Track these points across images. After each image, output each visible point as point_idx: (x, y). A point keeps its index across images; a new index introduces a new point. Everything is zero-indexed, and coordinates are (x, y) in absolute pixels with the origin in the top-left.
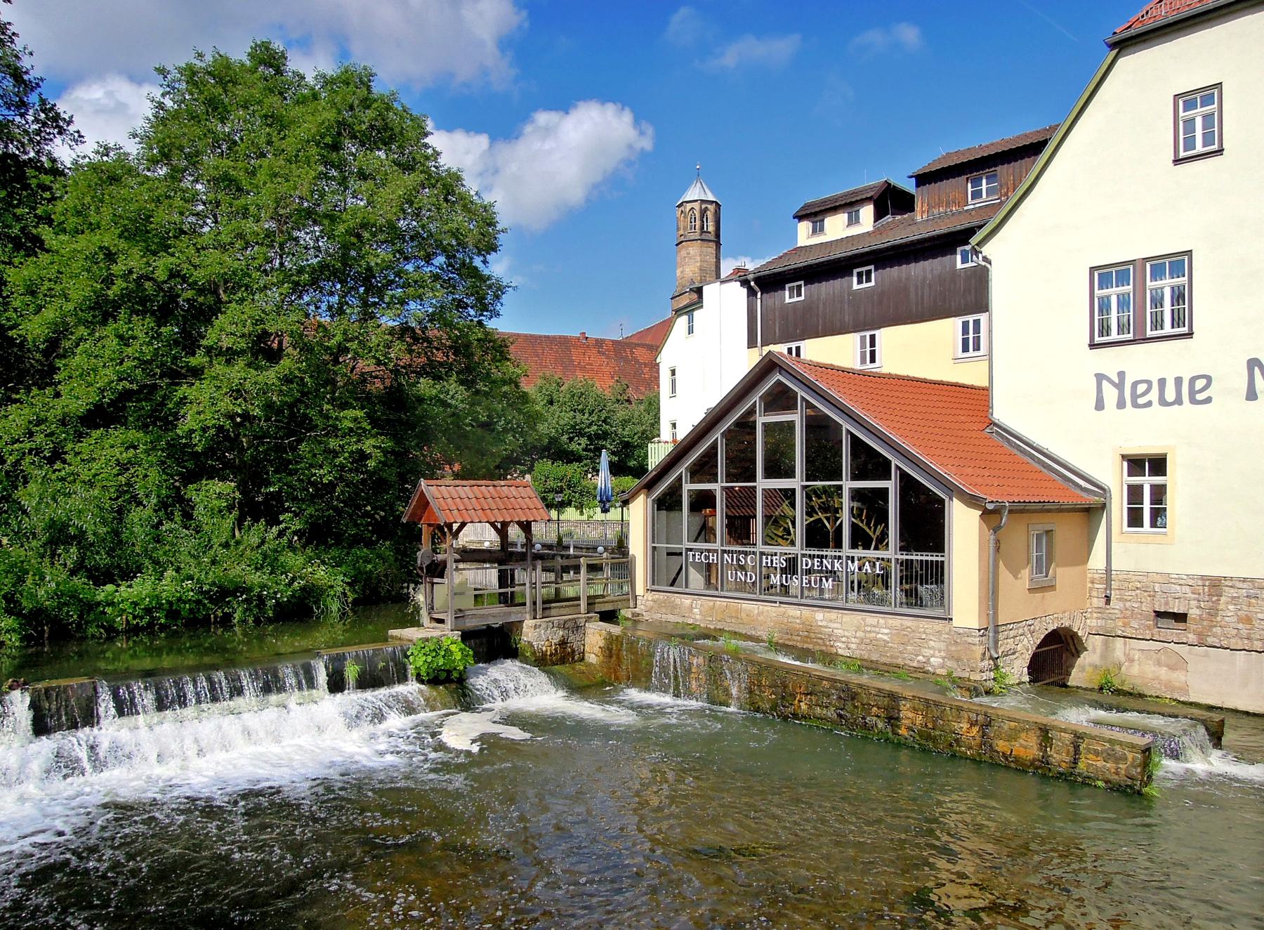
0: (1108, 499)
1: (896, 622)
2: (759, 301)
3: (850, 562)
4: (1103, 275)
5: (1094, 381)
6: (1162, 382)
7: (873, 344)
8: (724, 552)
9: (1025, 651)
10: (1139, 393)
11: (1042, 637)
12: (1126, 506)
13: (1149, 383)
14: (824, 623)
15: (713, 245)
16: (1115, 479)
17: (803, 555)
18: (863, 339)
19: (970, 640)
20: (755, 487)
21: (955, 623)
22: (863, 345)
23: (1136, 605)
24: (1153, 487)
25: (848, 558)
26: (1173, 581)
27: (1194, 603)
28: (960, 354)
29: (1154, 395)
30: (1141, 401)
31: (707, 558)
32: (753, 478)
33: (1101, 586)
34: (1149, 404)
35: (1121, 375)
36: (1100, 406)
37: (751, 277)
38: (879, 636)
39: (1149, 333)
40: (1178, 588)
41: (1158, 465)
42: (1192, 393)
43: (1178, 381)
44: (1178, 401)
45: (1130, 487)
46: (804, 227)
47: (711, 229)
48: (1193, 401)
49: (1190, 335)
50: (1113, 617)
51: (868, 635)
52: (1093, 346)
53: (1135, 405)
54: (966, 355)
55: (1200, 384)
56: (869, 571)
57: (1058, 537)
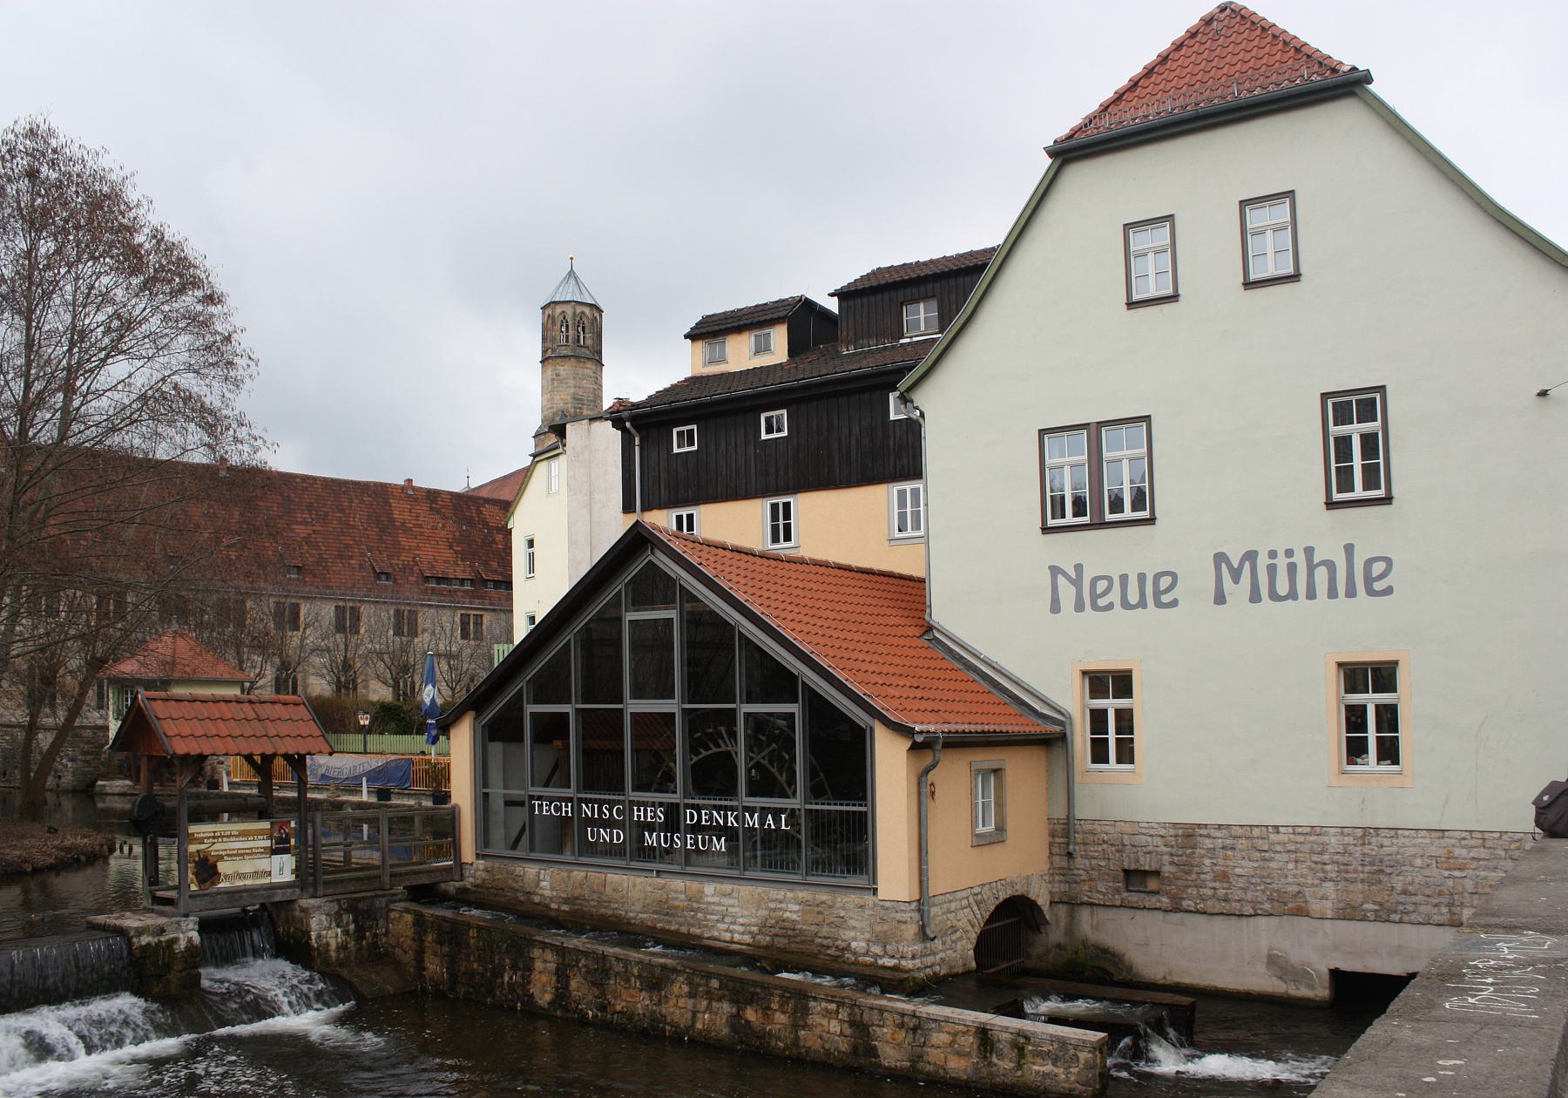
0: (1068, 727)
1: (803, 894)
3: (747, 814)
5: (1048, 574)
6: (1124, 579)
7: (787, 516)
8: (581, 800)
9: (970, 928)
10: (1099, 591)
11: (992, 908)
12: (1089, 736)
13: (1109, 579)
14: (715, 899)
16: (1072, 701)
17: (687, 806)
18: (774, 507)
19: (899, 916)
20: (622, 710)
21: (881, 894)
22: (775, 517)
23: (1103, 864)
24: (1118, 712)
25: (746, 809)
26: (1143, 831)
27: (1166, 858)
28: (897, 535)
29: (1116, 596)
31: (558, 809)
32: (619, 699)
33: (1062, 840)
34: (1110, 606)
35: (1079, 568)
36: (1055, 607)
38: (787, 915)
39: (1109, 517)
40: (1149, 839)
41: (1122, 683)
42: (1157, 594)
43: (1142, 578)
44: (1142, 603)
45: (1092, 711)
48: (1159, 604)
49: (1151, 520)
50: (1078, 879)
51: (772, 914)
52: (1046, 530)
53: (1095, 607)
55: (1165, 582)
56: (773, 827)
57: (1010, 776)
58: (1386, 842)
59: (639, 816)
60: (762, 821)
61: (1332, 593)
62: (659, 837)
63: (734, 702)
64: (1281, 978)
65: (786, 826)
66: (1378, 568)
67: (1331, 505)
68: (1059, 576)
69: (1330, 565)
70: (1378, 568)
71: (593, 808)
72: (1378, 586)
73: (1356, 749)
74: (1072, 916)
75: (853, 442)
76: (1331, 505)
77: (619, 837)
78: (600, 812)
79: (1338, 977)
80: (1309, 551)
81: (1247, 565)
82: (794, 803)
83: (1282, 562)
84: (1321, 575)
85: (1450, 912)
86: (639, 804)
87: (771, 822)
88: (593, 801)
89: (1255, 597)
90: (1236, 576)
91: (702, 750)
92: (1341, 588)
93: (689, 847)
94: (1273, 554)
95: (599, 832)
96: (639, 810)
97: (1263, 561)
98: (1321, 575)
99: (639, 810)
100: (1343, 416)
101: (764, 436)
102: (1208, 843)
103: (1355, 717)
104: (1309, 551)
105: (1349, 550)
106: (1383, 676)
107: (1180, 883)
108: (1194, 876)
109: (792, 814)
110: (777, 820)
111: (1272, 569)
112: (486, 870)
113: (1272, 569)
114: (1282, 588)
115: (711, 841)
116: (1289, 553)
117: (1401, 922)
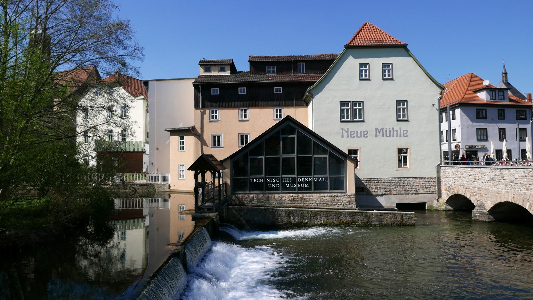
6: (357, 132)
13: (354, 131)
14: (307, 197)
29: (355, 135)
30: (352, 136)
34: (354, 137)
35: (348, 129)
36: (343, 137)
42: (364, 135)
43: (361, 132)
44: (361, 137)
48: (364, 137)
53: (351, 137)
59: (284, 181)
60: (318, 180)
61: (397, 136)
62: (290, 185)
66: (405, 132)
69: (397, 131)
70: (405, 132)
71: (270, 180)
72: (405, 135)
77: (278, 186)
78: (272, 180)
79: (398, 205)
80: (393, 128)
82: (327, 175)
83: (388, 130)
84: (395, 133)
86: (284, 178)
88: (270, 178)
89: (383, 136)
90: (379, 133)
92: (399, 135)
94: (386, 129)
95: (272, 185)
96: (284, 179)
97: (385, 130)
98: (395, 133)
99: (284, 179)
104: (393, 128)
105: (400, 128)
109: (326, 178)
110: (322, 180)
113: (386, 131)
114: (388, 135)
115: (305, 185)
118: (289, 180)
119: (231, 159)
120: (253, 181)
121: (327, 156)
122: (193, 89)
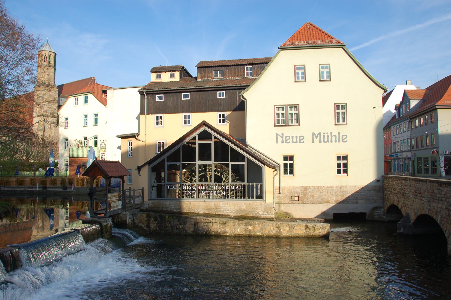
2: (146, 99)
4: (278, 107)
6: (293, 137)
10: (287, 139)
13: (289, 137)
14: (223, 206)
15: (53, 69)
16: (282, 162)
18: (185, 116)
29: (291, 140)
32: (195, 161)
34: (289, 142)
35: (283, 134)
36: (277, 142)
37: (145, 91)
39: (290, 124)
41: (291, 158)
42: (300, 140)
43: (296, 137)
44: (296, 142)
46: (154, 75)
47: (53, 62)
48: (300, 142)
53: (286, 142)
54: (220, 124)
55: (302, 138)
58: (345, 188)
60: (235, 187)
61: (336, 141)
63: (228, 162)
64: (324, 215)
65: (242, 188)
66: (344, 137)
67: (335, 124)
68: (278, 136)
69: (335, 136)
70: (344, 137)
72: (344, 140)
73: (339, 172)
74: (279, 206)
75: (208, 102)
76: (335, 124)
80: (331, 133)
81: (319, 135)
83: (326, 135)
84: (333, 138)
85: (356, 201)
87: (238, 188)
89: (320, 142)
90: (316, 138)
91: (217, 172)
93: (215, 194)
94: (324, 133)
97: (322, 135)
98: (333, 138)
100: (338, 107)
101: (183, 99)
102: (309, 190)
103: (339, 165)
104: (331, 133)
105: (339, 133)
106: (345, 157)
107: (303, 198)
108: (307, 197)
109: (244, 186)
111: (324, 137)
112: (152, 203)
113: (324, 137)
114: (326, 140)
116: (327, 133)
117: (347, 203)
118: (205, 187)
119: (149, 165)
120: (170, 187)
121: (245, 163)
122: (139, 96)
